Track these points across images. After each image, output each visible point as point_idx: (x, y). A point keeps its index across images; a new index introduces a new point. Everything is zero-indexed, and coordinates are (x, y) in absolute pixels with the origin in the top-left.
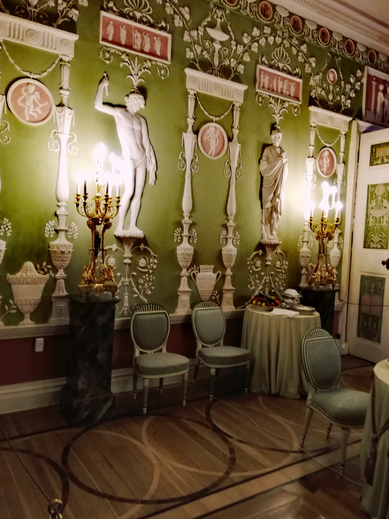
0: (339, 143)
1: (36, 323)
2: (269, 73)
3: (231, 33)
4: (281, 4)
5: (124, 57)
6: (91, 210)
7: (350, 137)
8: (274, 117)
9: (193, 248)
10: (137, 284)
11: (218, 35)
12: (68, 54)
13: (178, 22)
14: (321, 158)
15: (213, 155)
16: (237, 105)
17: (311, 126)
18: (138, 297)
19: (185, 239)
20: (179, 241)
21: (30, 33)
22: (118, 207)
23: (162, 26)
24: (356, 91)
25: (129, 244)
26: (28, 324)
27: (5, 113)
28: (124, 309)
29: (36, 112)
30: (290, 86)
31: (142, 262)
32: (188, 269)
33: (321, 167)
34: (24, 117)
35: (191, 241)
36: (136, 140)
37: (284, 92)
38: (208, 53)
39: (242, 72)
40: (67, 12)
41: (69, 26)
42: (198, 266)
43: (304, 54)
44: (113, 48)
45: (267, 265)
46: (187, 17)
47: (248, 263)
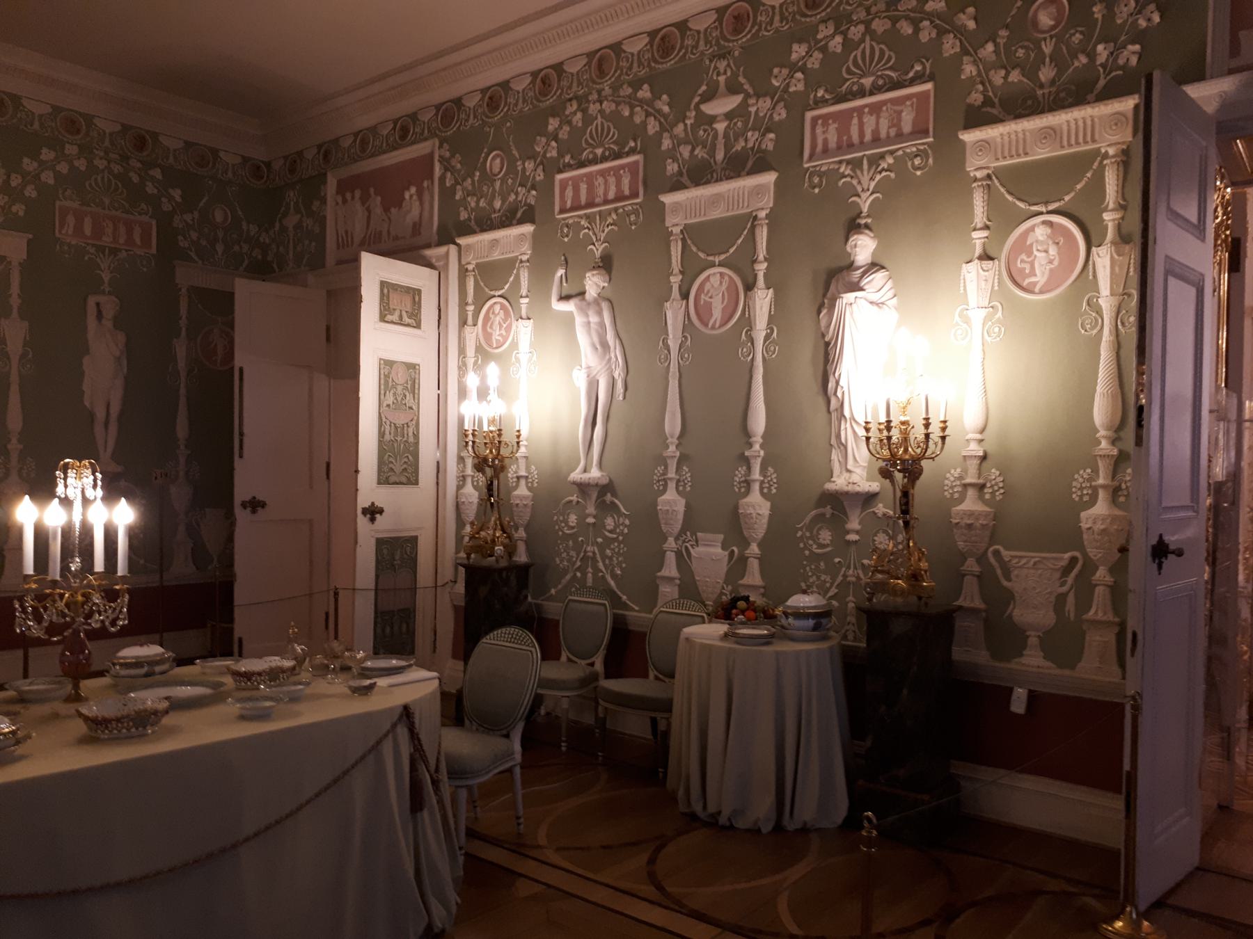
0: (1098, 184)
3: (747, 87)
8: (853, 202)
9: (683, 501)
10: (604, 557)
13: (653, 127)
14: (1023, 247)
17: (976, 180)
18: (603, 577)
19: (672, 486)
32: (676, 539)
34: (491, 346)
36: (591, 338)
39: (771, 147)
42: (694, 534)
45: (849, 543)
47: (799, 534)
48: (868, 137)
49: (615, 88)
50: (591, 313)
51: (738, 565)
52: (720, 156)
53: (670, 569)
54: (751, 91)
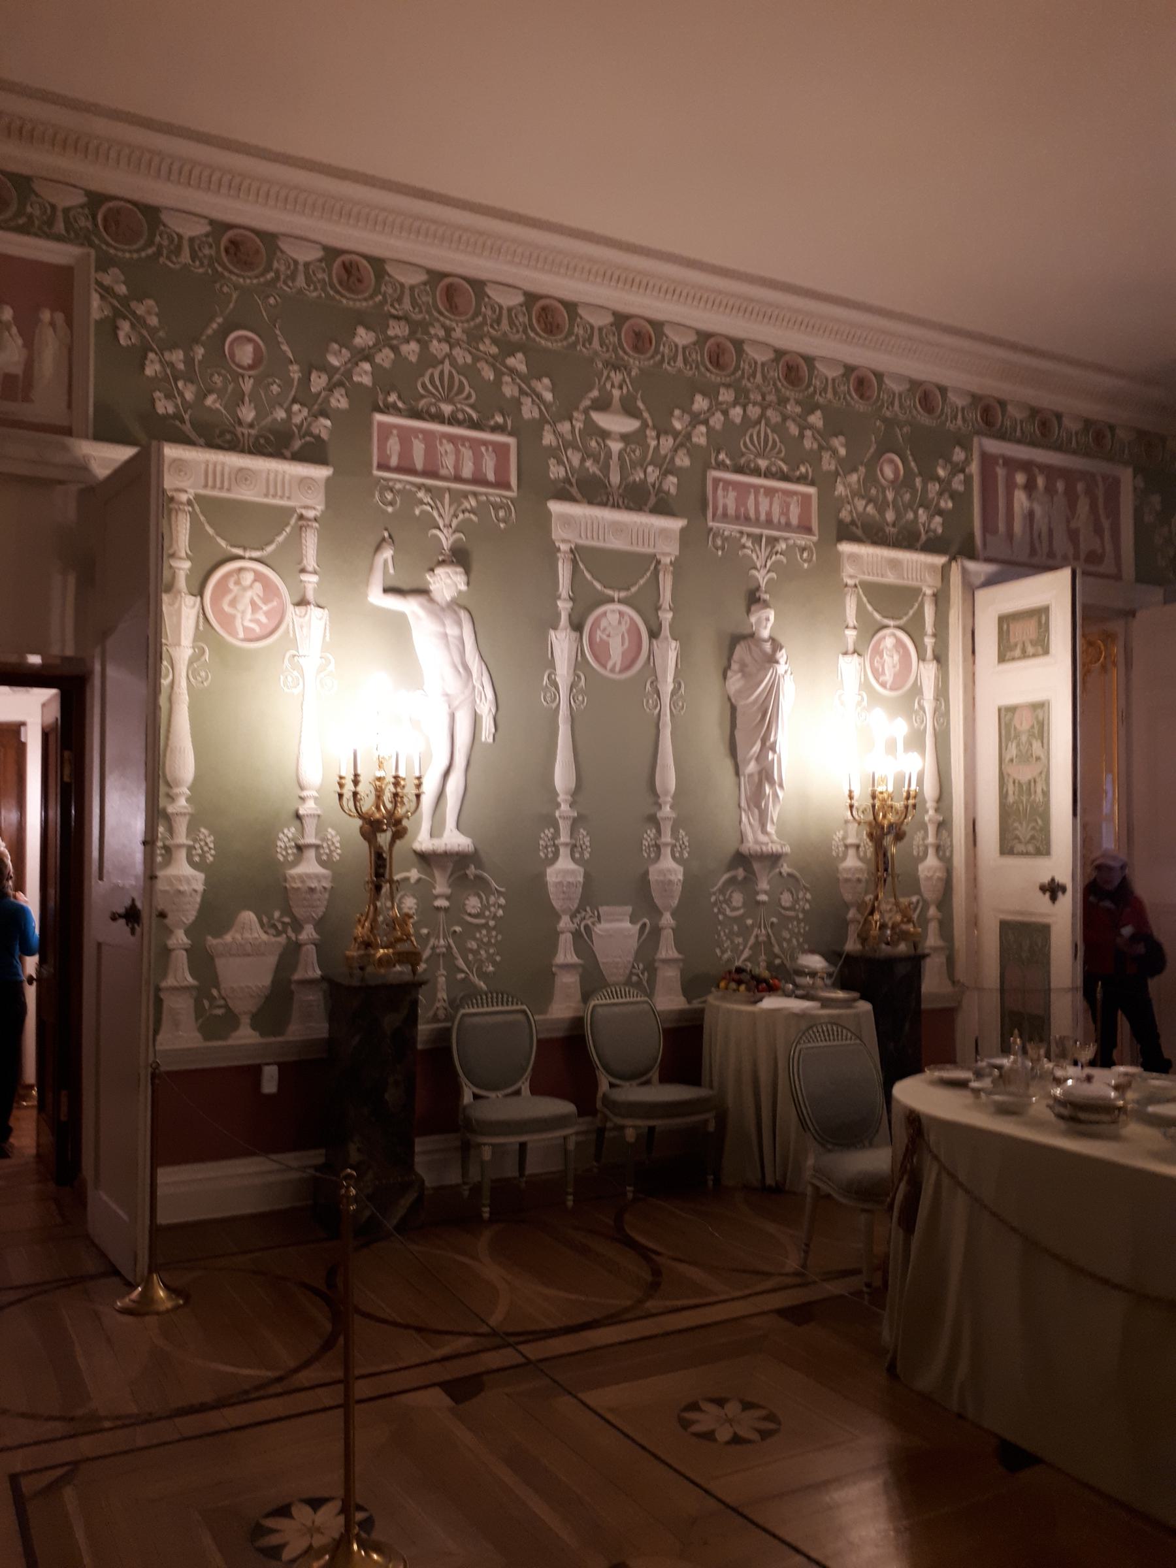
0: (920, 614)
1: (262, 1035)
2: (736, 485)
3: (646, 415)
4: (752, 337)
5: (421, 494)
6: (367, 805)
7: (948, 601)
9: (582, 870)
10: (464, 952)
11: (616, 423)
12: (314, 505)
13: (529, 411)
14: (877, 652)
15: (617, 669)
16: (666, 560)
17: (846, 585)
19: (564, 852)
20: (550, 855)
21: (242, 476)
22: (418, 796)
23: (496, 422)
24: (953, 496)
25: (443, 868)
26: (246, 1036)
27: (201, 628)
28: (438, 1005)
29: (257, 622)
30: (788, 506)
31: (473, 904)
32: (573, 917)
33: (877, 674)
34: (233, 633)
35: (577, 855)
37: (775, 520)
38: (596, 460)
39: (673, 490)
40: (310, 425)
41: (313, 453)
42: (595, 908)
43: (818, 432)
44: (400, 481)
45: (758, 903)
46: (548, 396)
47: (713, 899)
48: (763, 517)
49: (474, 337)
50: (448, 622)
51: (650, 938)
52: (615, 478)
53: (566, 954)
54: (650, 423)
